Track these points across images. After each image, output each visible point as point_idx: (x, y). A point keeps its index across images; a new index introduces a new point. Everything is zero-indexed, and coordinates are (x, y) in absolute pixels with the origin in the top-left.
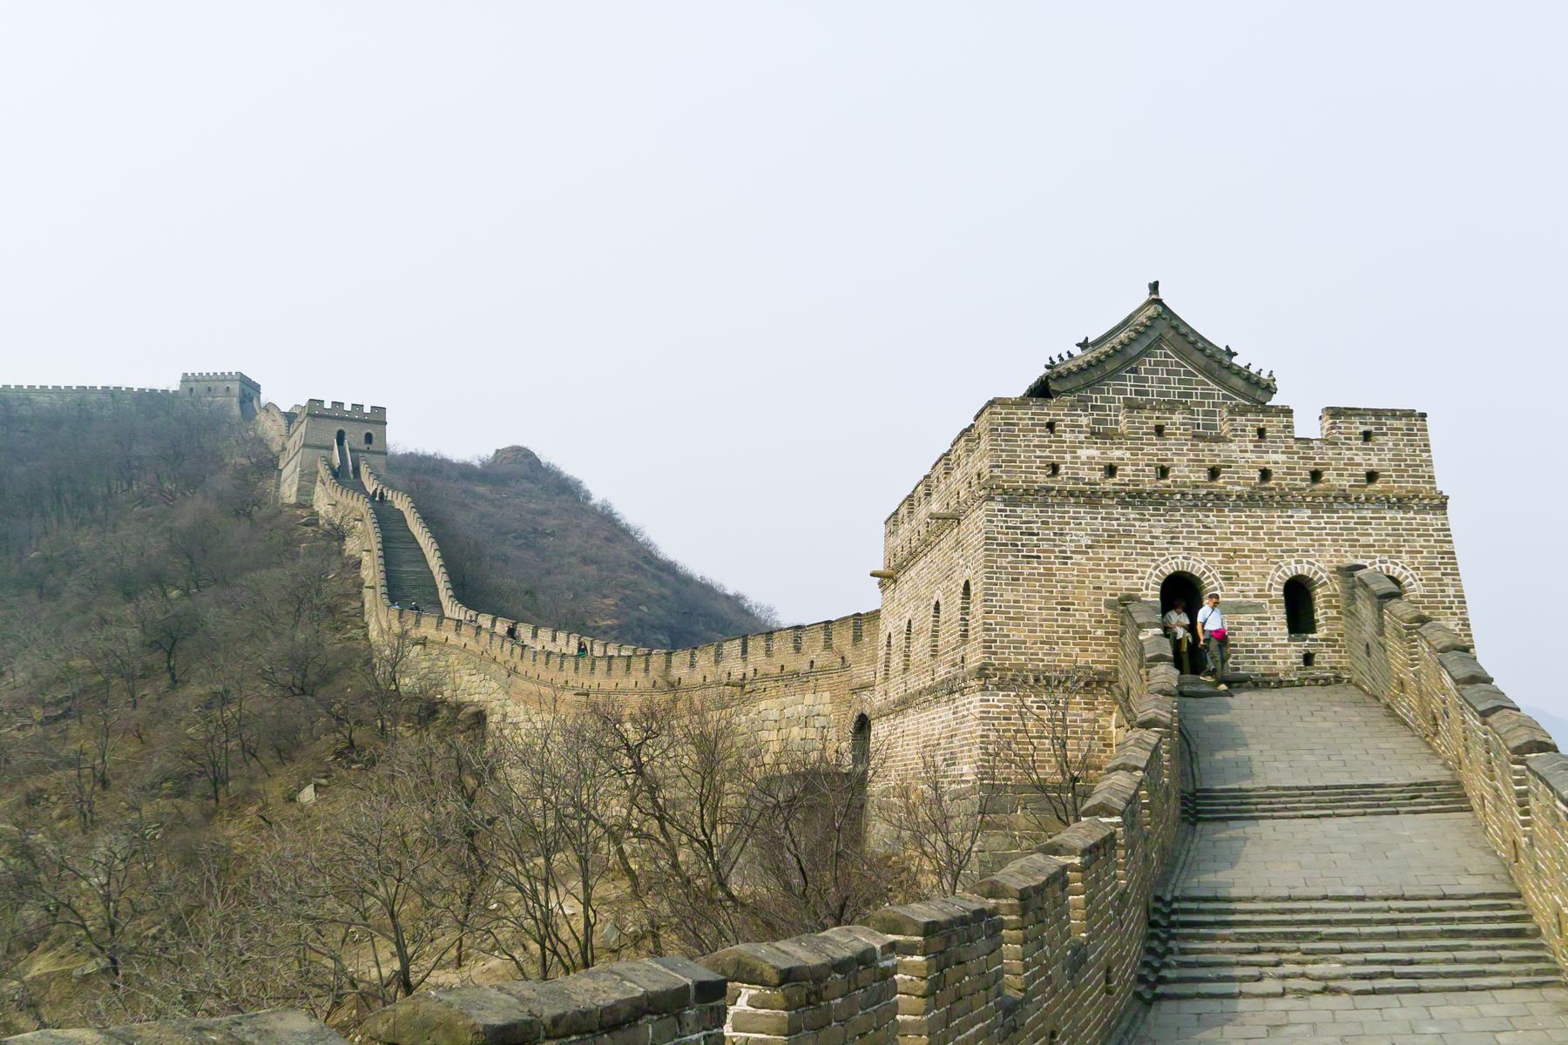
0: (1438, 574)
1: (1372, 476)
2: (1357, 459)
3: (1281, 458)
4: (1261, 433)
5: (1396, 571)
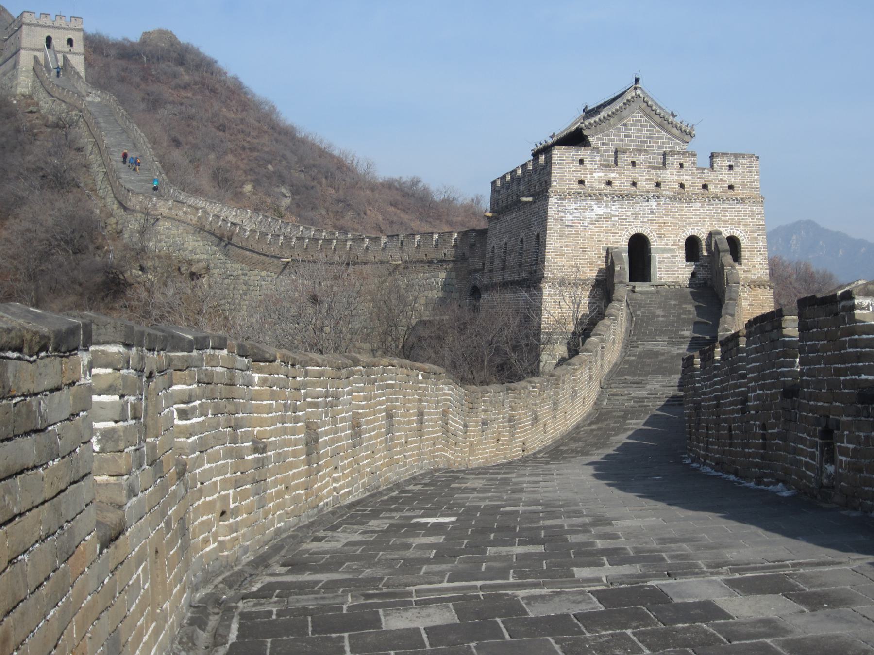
0: (756, 235)
1: (731, 187)
2: (725, 179)
3: (689, 178)
4: (681, 165)
5: (737, 234)
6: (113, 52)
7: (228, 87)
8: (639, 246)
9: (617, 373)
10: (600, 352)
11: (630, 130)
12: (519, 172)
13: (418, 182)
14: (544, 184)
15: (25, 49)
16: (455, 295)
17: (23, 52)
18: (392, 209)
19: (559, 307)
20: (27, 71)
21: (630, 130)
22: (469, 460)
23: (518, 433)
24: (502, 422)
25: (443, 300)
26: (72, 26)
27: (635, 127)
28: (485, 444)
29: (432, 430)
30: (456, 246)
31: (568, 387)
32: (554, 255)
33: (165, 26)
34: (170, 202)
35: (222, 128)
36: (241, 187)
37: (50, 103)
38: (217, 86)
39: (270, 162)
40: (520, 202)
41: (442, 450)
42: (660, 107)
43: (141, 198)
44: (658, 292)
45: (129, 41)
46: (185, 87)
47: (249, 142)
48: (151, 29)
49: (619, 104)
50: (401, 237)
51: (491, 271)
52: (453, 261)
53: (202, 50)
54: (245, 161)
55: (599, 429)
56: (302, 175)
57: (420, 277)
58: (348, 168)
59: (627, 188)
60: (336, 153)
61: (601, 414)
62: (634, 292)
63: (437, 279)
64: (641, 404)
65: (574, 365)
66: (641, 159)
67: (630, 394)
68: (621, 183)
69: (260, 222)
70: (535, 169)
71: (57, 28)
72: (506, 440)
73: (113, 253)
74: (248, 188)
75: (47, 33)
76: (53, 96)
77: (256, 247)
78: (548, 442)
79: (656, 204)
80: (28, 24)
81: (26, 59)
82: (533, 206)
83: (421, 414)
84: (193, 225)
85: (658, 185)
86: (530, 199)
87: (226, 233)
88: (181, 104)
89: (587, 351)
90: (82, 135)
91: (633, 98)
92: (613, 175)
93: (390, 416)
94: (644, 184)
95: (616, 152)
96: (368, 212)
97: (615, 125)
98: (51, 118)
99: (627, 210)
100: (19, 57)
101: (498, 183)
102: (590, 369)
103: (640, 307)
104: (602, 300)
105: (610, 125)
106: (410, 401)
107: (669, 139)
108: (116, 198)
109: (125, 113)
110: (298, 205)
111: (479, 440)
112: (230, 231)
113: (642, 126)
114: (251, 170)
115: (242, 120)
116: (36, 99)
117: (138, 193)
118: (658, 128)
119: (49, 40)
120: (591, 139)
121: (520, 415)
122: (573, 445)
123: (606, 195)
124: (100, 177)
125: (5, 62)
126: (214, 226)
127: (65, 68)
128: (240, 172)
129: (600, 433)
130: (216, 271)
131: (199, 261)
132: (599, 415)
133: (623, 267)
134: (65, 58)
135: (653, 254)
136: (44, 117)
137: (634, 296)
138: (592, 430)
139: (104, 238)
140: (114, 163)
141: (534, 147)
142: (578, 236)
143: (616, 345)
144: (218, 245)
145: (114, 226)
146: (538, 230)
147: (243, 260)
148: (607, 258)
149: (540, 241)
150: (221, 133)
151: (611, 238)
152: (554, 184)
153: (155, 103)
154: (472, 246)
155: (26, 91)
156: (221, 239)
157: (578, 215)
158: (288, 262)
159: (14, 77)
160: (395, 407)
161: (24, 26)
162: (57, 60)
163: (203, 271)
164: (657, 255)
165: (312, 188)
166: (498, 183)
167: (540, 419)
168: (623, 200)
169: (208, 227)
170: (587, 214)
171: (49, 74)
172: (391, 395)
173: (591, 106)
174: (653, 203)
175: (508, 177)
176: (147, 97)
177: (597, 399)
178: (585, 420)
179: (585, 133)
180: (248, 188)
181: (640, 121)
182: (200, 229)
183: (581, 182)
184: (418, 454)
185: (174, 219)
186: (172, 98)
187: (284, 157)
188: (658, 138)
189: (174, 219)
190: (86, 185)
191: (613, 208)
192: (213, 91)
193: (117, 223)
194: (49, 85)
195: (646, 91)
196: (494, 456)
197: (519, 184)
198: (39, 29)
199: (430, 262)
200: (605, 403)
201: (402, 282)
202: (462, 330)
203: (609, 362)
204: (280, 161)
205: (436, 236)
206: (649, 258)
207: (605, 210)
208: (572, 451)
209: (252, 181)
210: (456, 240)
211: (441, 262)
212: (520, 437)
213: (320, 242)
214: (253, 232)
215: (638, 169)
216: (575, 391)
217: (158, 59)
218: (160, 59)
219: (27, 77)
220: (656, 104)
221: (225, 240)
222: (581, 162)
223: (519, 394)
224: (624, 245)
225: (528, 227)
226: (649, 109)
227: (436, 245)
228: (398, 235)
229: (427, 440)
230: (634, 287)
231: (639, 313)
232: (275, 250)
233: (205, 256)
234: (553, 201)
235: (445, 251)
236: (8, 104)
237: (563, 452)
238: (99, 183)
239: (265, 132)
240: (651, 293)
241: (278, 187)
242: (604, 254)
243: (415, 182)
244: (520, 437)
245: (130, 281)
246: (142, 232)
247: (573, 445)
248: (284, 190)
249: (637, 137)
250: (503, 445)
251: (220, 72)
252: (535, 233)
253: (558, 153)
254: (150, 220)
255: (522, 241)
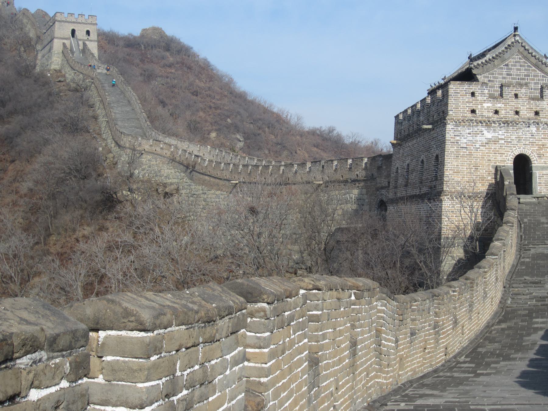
6: (121, 43)
7: (200, 66)
8: (522, 164)
9: (515, 275)
10: (502, 255)
11: (511, 69)
12: (419, 106)
13: (333, 130)
14: (441, 114)
15: (57, 38)
16: (366, 208)
17: (55, 40)
18: (315, 149)
19: (457, 216)
20: (58, 53)
21: (511, 69)
22: (399, 376)
23: (442, 338)
24: (428, 330)
25: (356, 211)
26: (89, 21)
27: (516, 67)
28: (414, 354)
29: (366, 358)
30: (366, 169)
31: (480, 289)
32: (451, 172)
33: (156, 25)
34: (151, 141)
35: (195, 93)
36: (208, 134)
37: (73, 74)
38: (192, 64)
39: (229, 117)
40: (420, 129)
41: (376, 377)
42: (535, 51)
43: (130, 138)
44: (539, 203)
45: (132, 35)
46: (170, 66)
47: (214, 103)
48: (147, 27)
49: (501, 48)
50: (323, 163)
51: (396, 187)
52: (364, 180)
53: (182, 40)
54: (211, 116)
55: (509, 328)
56: (252, 126)
57: (335, 193)
58: (284, 121)
59: (511, 116)
60: (275, 110)
61: (507, 313)
62: (519, 203)
63: (351, 195)
64: (543, 303)
65: (484, 268)
66: (522, 91)
67: (532, 294)
68: (507, 112)
69: (217, 155)
70: (433, 102)
71: (79, 23)
72: (431, 348)
73: (110, 178)
74: (213, 135)
75: (72, 27)
76: (74, 70)
77: (214, 173)
78: (465, 343)
79: (535, 129)
80: (59, 21)
81: (57, 45)
82: (432, 132)
83: (354, 344)
84: (167, 158)
85: (537, 113)
86: (430, 127)
87: (191, 163)
88: (167, 77)
89: (493, 254)
90: (93, 95)
91: (512, 43)
92: (499, 105)
93: (314, 362)
94: (526, 113)
95: (502, 87)
96: (298, 152)
97: (498, 65)
98: (73, 85)
99: (512, 134)
100: (53, 44)
101: (401, 117)
102: (496, 270)
103: (526, 216)
104: (492, 210)
105: (494, 65)
106: (341, 333)
107: (543, 76)
108: (113, 139)
109: (123, 79)
110: (249, 147)
111: (409, 352)
112: (193, 161)
113: (521, 66)
114: (215, 122)
115: (209, 88)
116: (63, 73)
117: (128, 135)
118: (533, 68)
119: (73, 32)
120: (479, 77)
121: (443, 320)
122: (490, 347)
123: (494, 122)
124: (104, 124)
125: (44, 48)
126: (183, 158)
127: (85, 50)
128: (208, 124)
129: (511, 332)
130: (183, 192)
131: (171, 184)
132: (505, 314)
133: (509, 181)
134: (84, 44)
135: (534, 171)
136: (68, 84)
137: (520, 206)
138: (503, 329)
139: (104, 168)
140: (113, 114)
141: (429, 87)
142: (472, 158)
143: (513, 248)
144: (185, 172)
145: (111, 159)
146: (437, 152)
147: (203, 183)
148: (496, 174)
149: (439, 161)
150: (195, 97)
151: (499, 158)
152: (450, 113)
153: (149, 77)
154: (379, 168)
155: (57, 67)
156: (187, 167)
157: (471, 139)
158: (237, 184)
159: (50, 57)
160: (322, 348)
161: (56, 23)
162: (78, 45)
163: (174, 192)
164: (537, 172)
165: (259, 134)
166: (401, 117)
167: (459, 322)
168: (508, 126)
169: (178, 159)
170: (478, 138)
171: (73, 55)
172: (317, 331)
173: (475, 54)
174: (533, 129)
175: (409, 111)
176: (143, 72)
177: (502, 298)
178: (493, 318)
179: (474, 72)
180: (213, 135)
181: (519, 62)
182: (173, 160)
183: (473, 111)
184: (351, 397)
185: (154, 154)
186: (161, 74)
187: (238, 113)
188: (534, 76)
189: (154, 154)
190: (94, 131)
191: (500, 132)
192: (190, 68)
193: (114, 157)
194: (72, 62)
195: (524, 38)
196: (421, 366)
197: (419, 116)
198: (66, 24)
199: (346, 182)
200: (509, 302)
201: (324, 197)
202: (375, 235)
203: (509, 264)
204: (236, 116)
205: (350, 161)
206: (531, 175)
207: (493, 134)
208: (492, 354)
209: (216, 130)
210: (366, 164)
211: (354, 181)
212: (443, 343)
213: (260, 168)
214: (211, 161)
215: (520, 100)
216: (485, 293)
217: (152, 47)
218: (153, 47)
219: (59, 57)
220: (532, 48)
221: (190, 168)
222: (473, 94)
223: (443, 300)
224: (510, 164)
225: (428, 150)
226: (527, 52)
227: (350, 168)
228: (320, 161)
229: (360, 373)
230: (519, 199)
231: (525, 220)
232: (226, 174)
233: (176, 180)
234: (449, 127)
235: (358, 173)
236: (44, 76)
237: (484, 356)
238: (103, 129)
239: (226, 96)
240: (534, 203)
241: (235, 134)
242: (493, 172)
243: (331, 130)
244: (443, 342)
245: (122, 199)
246: (131, 163)
247: (490, 347)
248: (238, 137)
249: (517, 75)
250: (429, 353)
251: (195, 55)
252: (435, 155)
253: (453, 87)
254: (136, 154)
255: (422, 162)
